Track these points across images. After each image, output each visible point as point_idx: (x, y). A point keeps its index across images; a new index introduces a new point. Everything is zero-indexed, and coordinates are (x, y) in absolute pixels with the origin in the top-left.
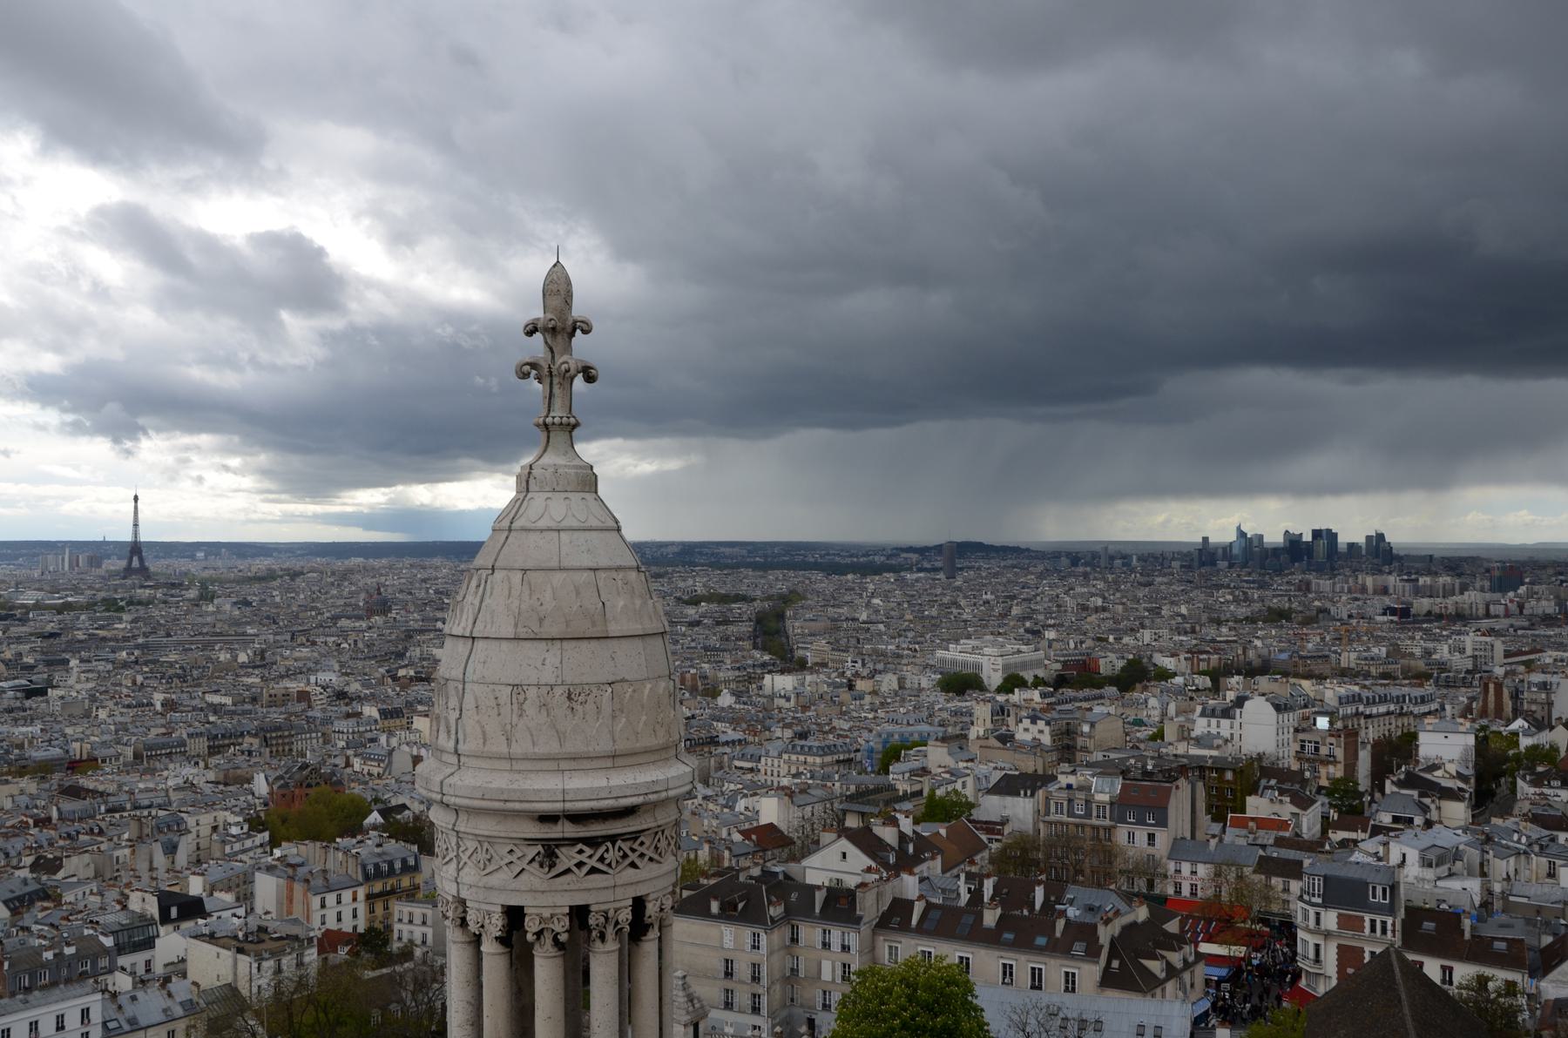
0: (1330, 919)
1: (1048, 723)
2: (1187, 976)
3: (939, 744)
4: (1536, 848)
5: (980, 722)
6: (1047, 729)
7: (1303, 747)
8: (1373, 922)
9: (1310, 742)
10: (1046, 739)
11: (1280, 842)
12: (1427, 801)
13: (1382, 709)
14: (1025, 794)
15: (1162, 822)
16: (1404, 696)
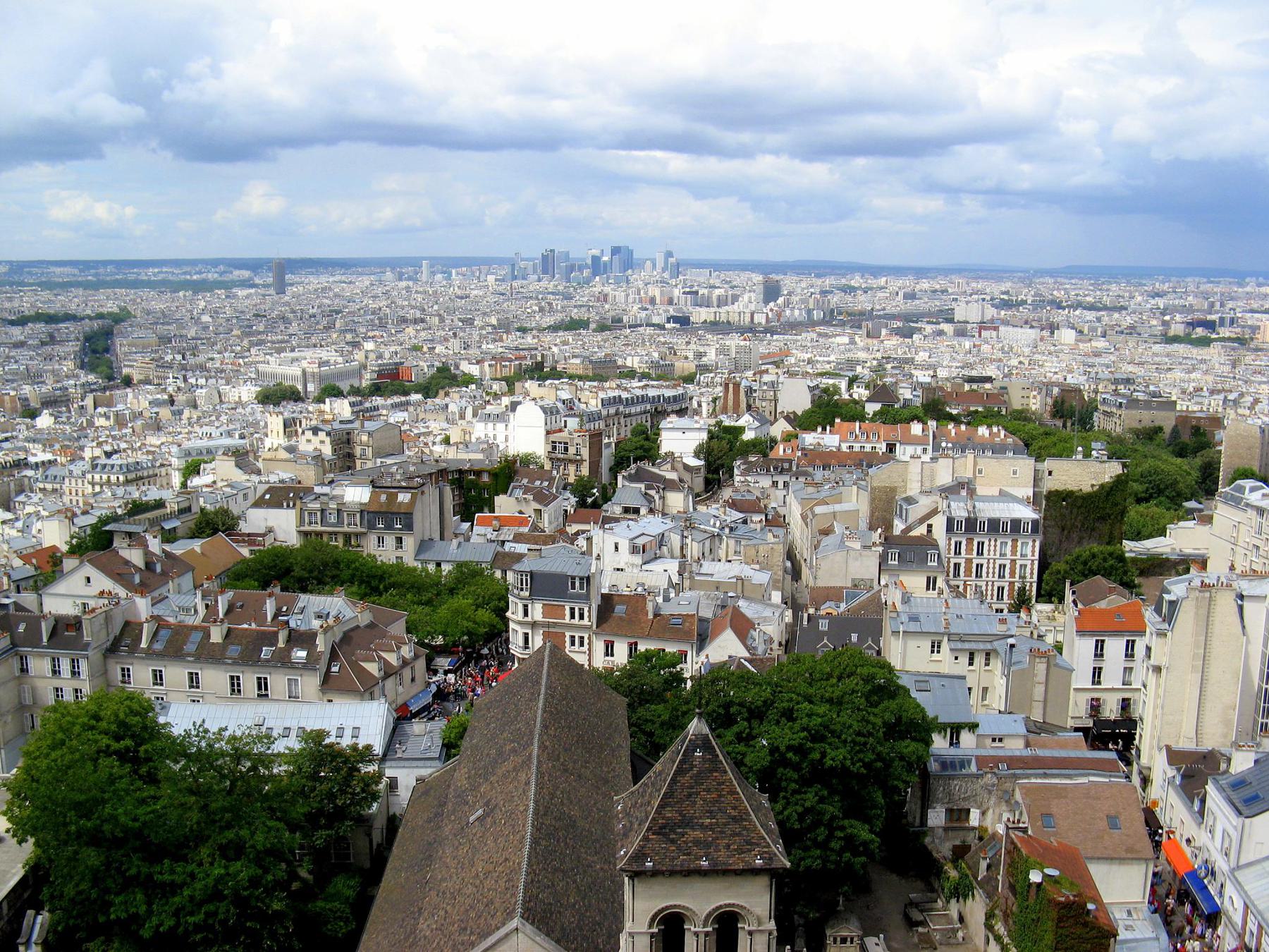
0: (537, 611)
1: (328, 434)
2: (407, 673)
3: (226, 458)
4: (727, 530)
5: (275, 433)
6: (328, 440)
7: (554, 448)
8: (572, 610)
9: (560, 443)
10: (327, 450)
11: (518, 538)
12: (652, 492)
13: (638, 409)
14: (288, 506)
15: (409, 527)
16: (659, 396)
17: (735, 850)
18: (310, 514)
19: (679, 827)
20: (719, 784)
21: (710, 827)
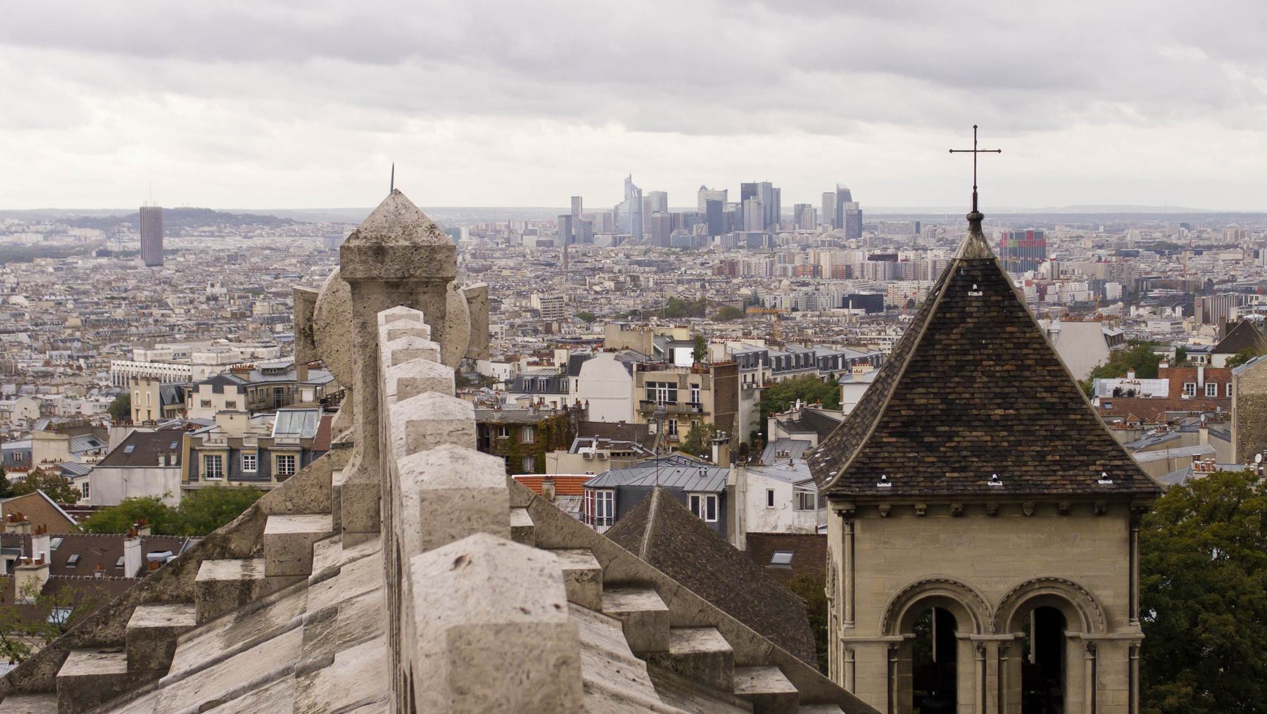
1: (243, 390)
7: (651, 395)
9: (662, 385)
14: (168, 463)
16: (835, 358)
17: (1055, 463)
18: (209, 458)
19: (943, 423)
20: (1019, 346)
21: (1003, 423)
